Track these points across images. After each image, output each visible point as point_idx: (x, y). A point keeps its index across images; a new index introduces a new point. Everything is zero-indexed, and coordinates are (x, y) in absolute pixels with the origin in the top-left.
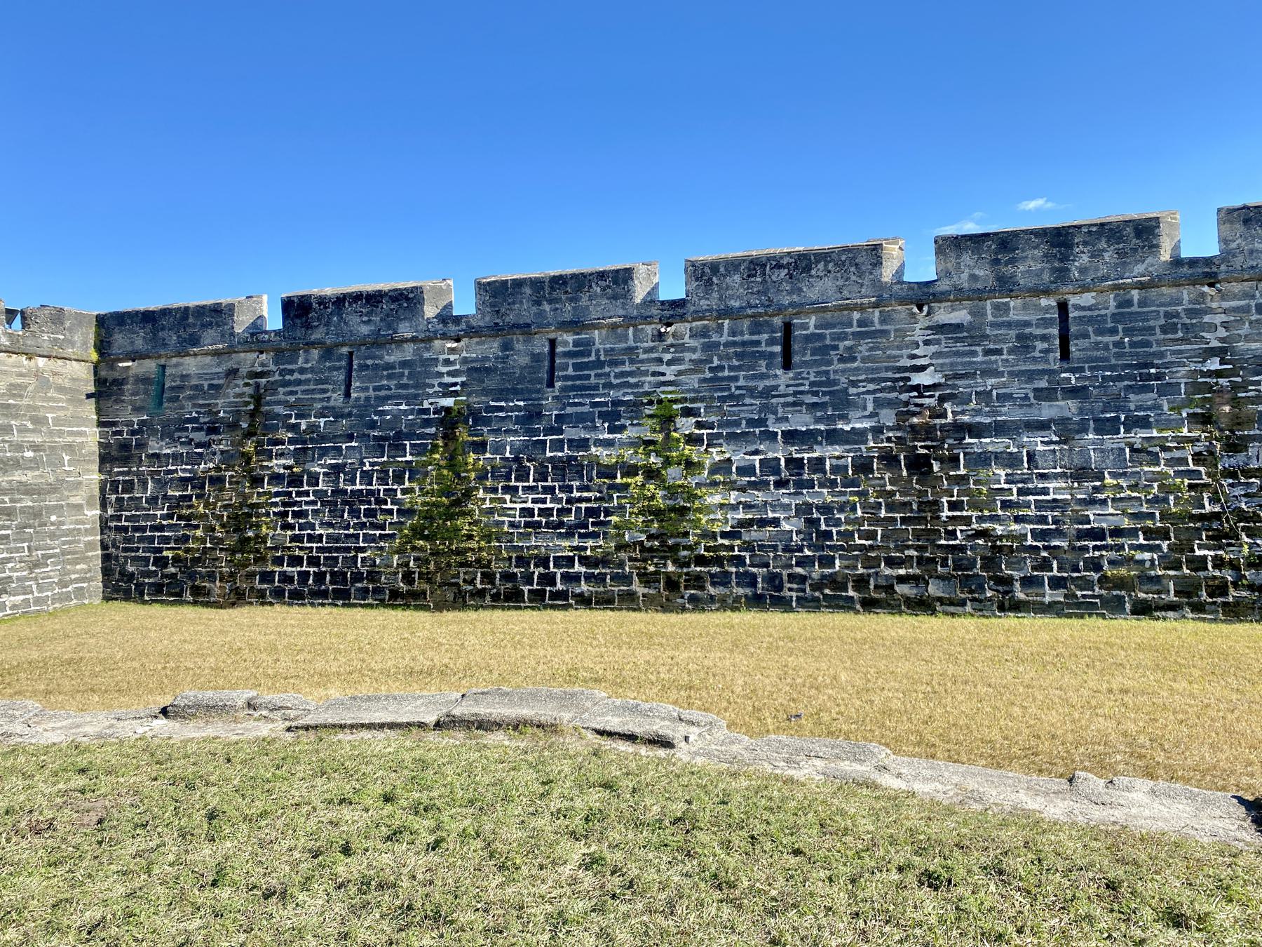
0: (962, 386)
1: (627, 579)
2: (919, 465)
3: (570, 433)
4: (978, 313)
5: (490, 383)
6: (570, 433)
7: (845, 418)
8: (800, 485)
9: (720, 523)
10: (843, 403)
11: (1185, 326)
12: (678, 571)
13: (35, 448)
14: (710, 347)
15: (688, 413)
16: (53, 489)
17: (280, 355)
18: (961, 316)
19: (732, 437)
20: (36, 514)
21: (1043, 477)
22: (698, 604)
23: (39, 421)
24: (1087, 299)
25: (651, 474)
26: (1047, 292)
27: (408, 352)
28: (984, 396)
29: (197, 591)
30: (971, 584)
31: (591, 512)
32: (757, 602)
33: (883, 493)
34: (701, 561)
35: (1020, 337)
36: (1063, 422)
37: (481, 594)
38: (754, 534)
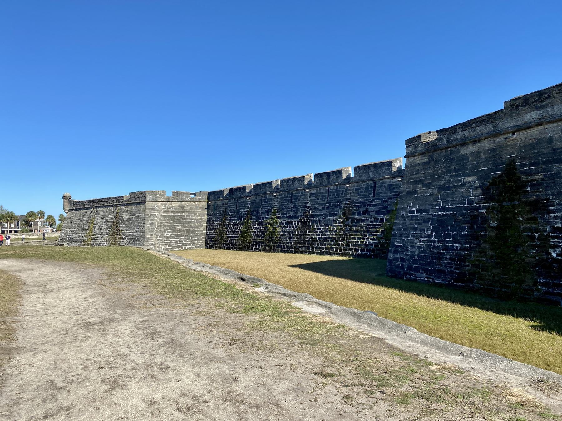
0: (313, 207)
1: (265, 246)
2: (305, 223)
4: (317, 191)
5: (254, 206)
6: (263, 216)
7: (297, 213)
8: (290, 227)
9: (278, 235)
10: (297, 210)
12: (272, 245)
13: (194, 219)
14: (282, 198)
15: (278, 212)
16: (197, 227)
17: (230, 200)
18: (314, 191)
20: (193, 232)
21: (321, 226)
22: (274, 251)
23: (195, 214)
24: (331, 188)
25: (272, 225)
26: (326, 186)
27: (243, 200)
28: (315, 208)
29: (216, 247)
30: (309, 248)
31: (263, 232)
32: (282, 251)
33: (300, 229)
34: (276, 243)
35: (322, 196)
36: (325, 214)
37: (248, 248)
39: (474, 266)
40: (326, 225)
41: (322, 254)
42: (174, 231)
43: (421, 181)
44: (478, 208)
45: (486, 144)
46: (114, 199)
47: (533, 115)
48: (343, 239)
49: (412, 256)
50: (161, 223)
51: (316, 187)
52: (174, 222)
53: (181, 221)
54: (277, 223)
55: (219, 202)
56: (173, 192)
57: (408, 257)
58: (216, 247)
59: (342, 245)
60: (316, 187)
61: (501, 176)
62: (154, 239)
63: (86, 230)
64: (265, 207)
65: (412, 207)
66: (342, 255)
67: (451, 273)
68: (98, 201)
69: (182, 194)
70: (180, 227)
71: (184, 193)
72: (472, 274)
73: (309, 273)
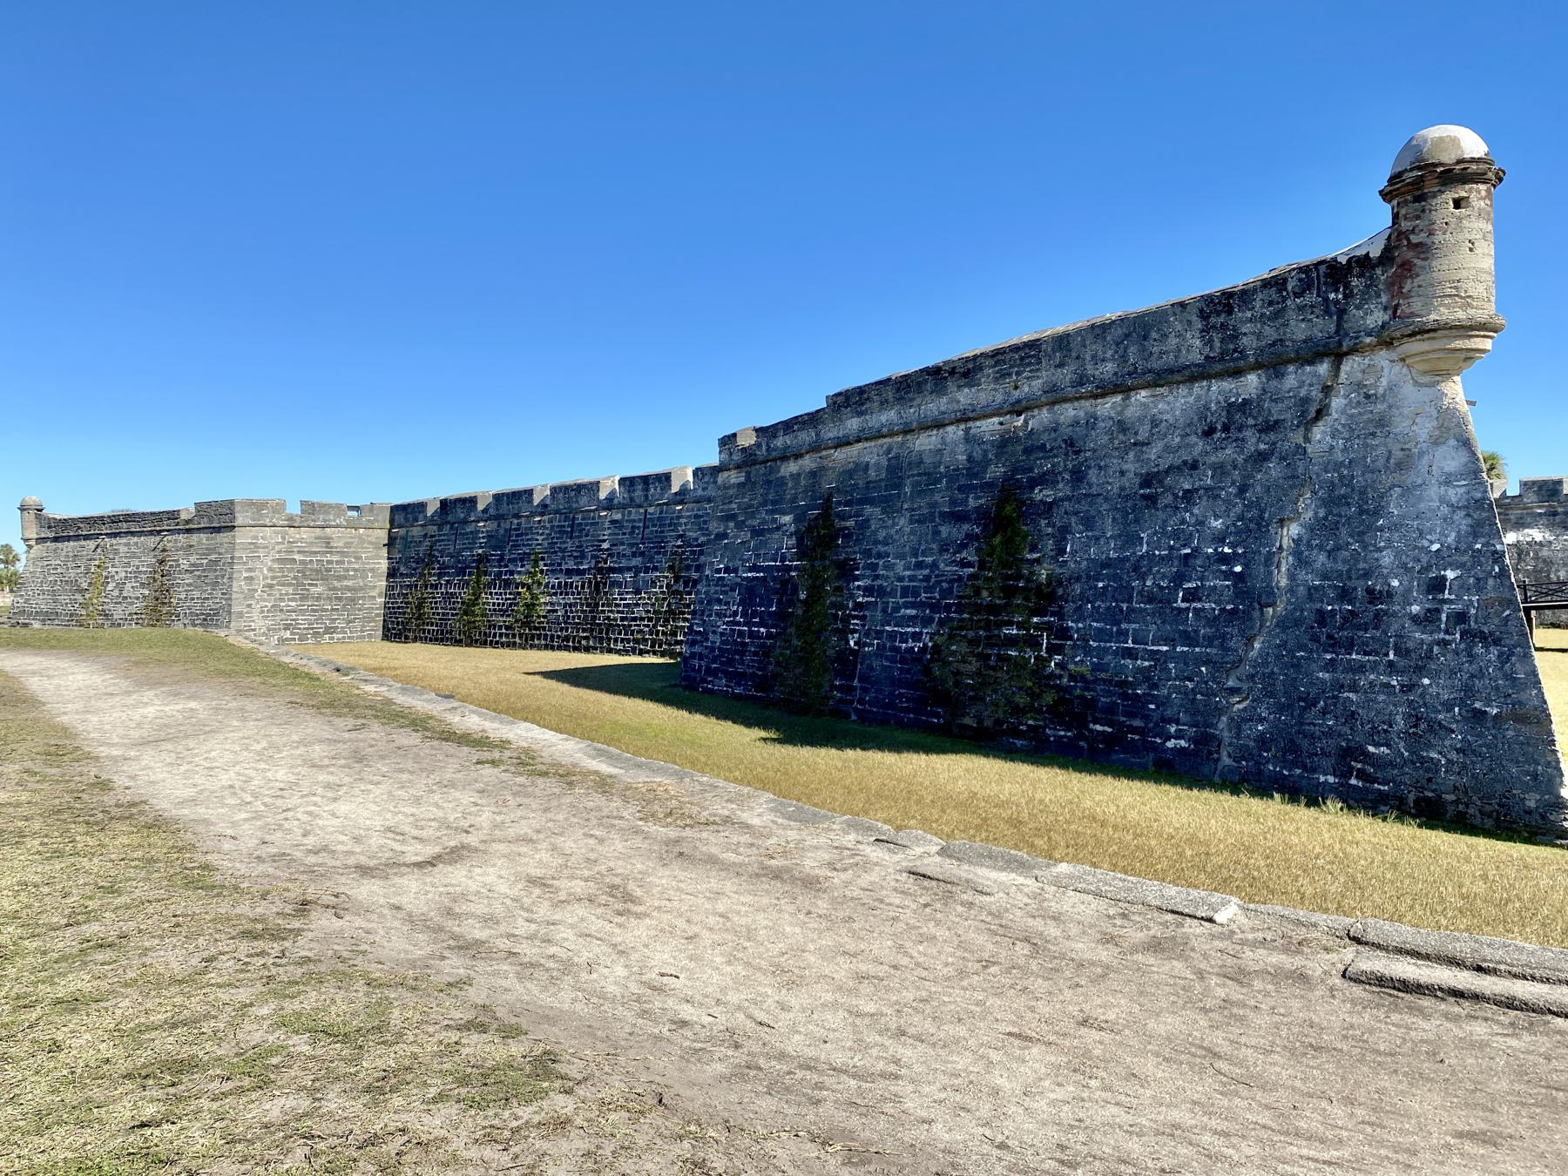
3: (511, 567)
5: (493, 542)
6: (511, 567)
10: (583, 556)
11: (674, 525)
13: (355, 570)
16: (361, 589)
17: (440, 527)
18: (618, 516)
19: (553, 571)
20: (353, 600)
22: (532, 647)
23: (358, 558)
24: (651, 510)
32: (546, 647)
34: (536, 629)
38: (552, 616)
39: (778, 664)
40: (637, 592)
41: (626, 652)
42: (304, 598)
43: (732, 517)
44: (790, 568)
45: (808, 463)
46: (157, 517)
47: (853, 424)
48: (666, 620)
49: (712, 649)
50: (273, 578)
51: (622, 507)
52: (304, 576)
53: (322, 574)
54: (540, 584)
55: (416, 532)
56: (303, 503)
58: (407, 637)
59: (664, 633)
60: (622, 507)
61: (816, 519)
62: (255, 615)
63: (82, 591)
64: (516, 546)
66: (663, 654)
67: (753, 675)
68: (114, 519)
69: (326, 508)
70: (320, 589)
71: (330, 506)
72: (775, 676)
73: (553, 684)
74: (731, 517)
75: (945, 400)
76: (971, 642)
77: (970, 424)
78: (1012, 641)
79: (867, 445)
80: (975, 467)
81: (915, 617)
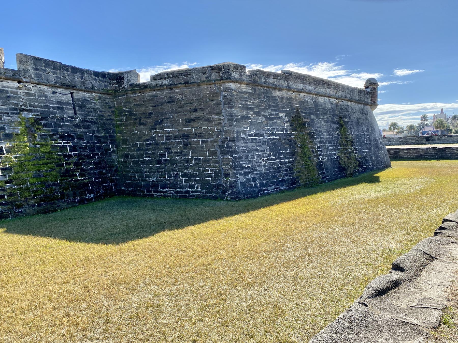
44: (290, 135)
47: (301, 86)
49: (261, 174)
57: (258, 176)
65: (250, 131)
67: (288, 179)
72: (298, 177)
74: (249, 108)
75: (324, 90)
76: (345, 154)
77: (330, 99)
78: (350, 152)
79: (305, 94)
80: (333, 110)
81: (333, 149)
